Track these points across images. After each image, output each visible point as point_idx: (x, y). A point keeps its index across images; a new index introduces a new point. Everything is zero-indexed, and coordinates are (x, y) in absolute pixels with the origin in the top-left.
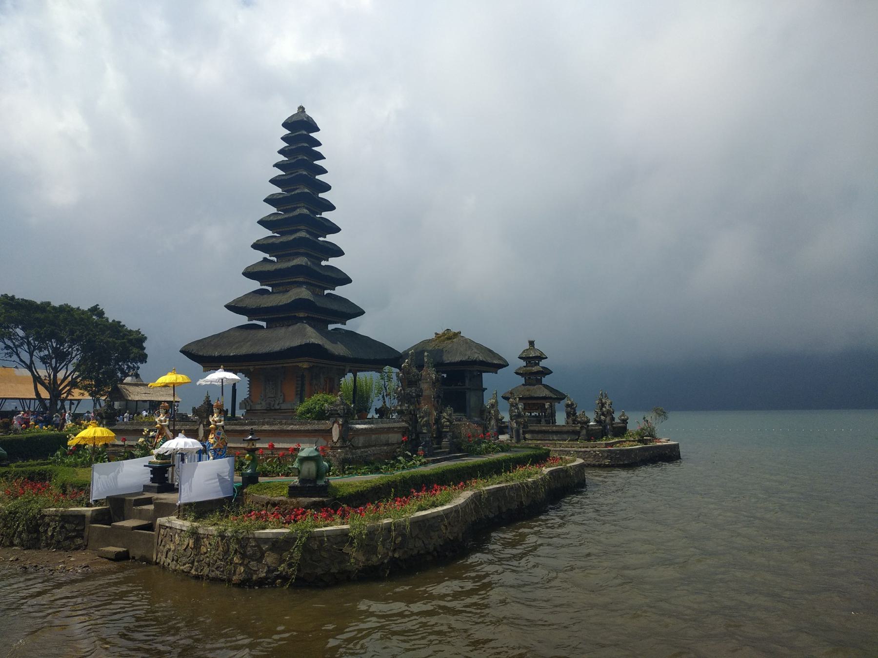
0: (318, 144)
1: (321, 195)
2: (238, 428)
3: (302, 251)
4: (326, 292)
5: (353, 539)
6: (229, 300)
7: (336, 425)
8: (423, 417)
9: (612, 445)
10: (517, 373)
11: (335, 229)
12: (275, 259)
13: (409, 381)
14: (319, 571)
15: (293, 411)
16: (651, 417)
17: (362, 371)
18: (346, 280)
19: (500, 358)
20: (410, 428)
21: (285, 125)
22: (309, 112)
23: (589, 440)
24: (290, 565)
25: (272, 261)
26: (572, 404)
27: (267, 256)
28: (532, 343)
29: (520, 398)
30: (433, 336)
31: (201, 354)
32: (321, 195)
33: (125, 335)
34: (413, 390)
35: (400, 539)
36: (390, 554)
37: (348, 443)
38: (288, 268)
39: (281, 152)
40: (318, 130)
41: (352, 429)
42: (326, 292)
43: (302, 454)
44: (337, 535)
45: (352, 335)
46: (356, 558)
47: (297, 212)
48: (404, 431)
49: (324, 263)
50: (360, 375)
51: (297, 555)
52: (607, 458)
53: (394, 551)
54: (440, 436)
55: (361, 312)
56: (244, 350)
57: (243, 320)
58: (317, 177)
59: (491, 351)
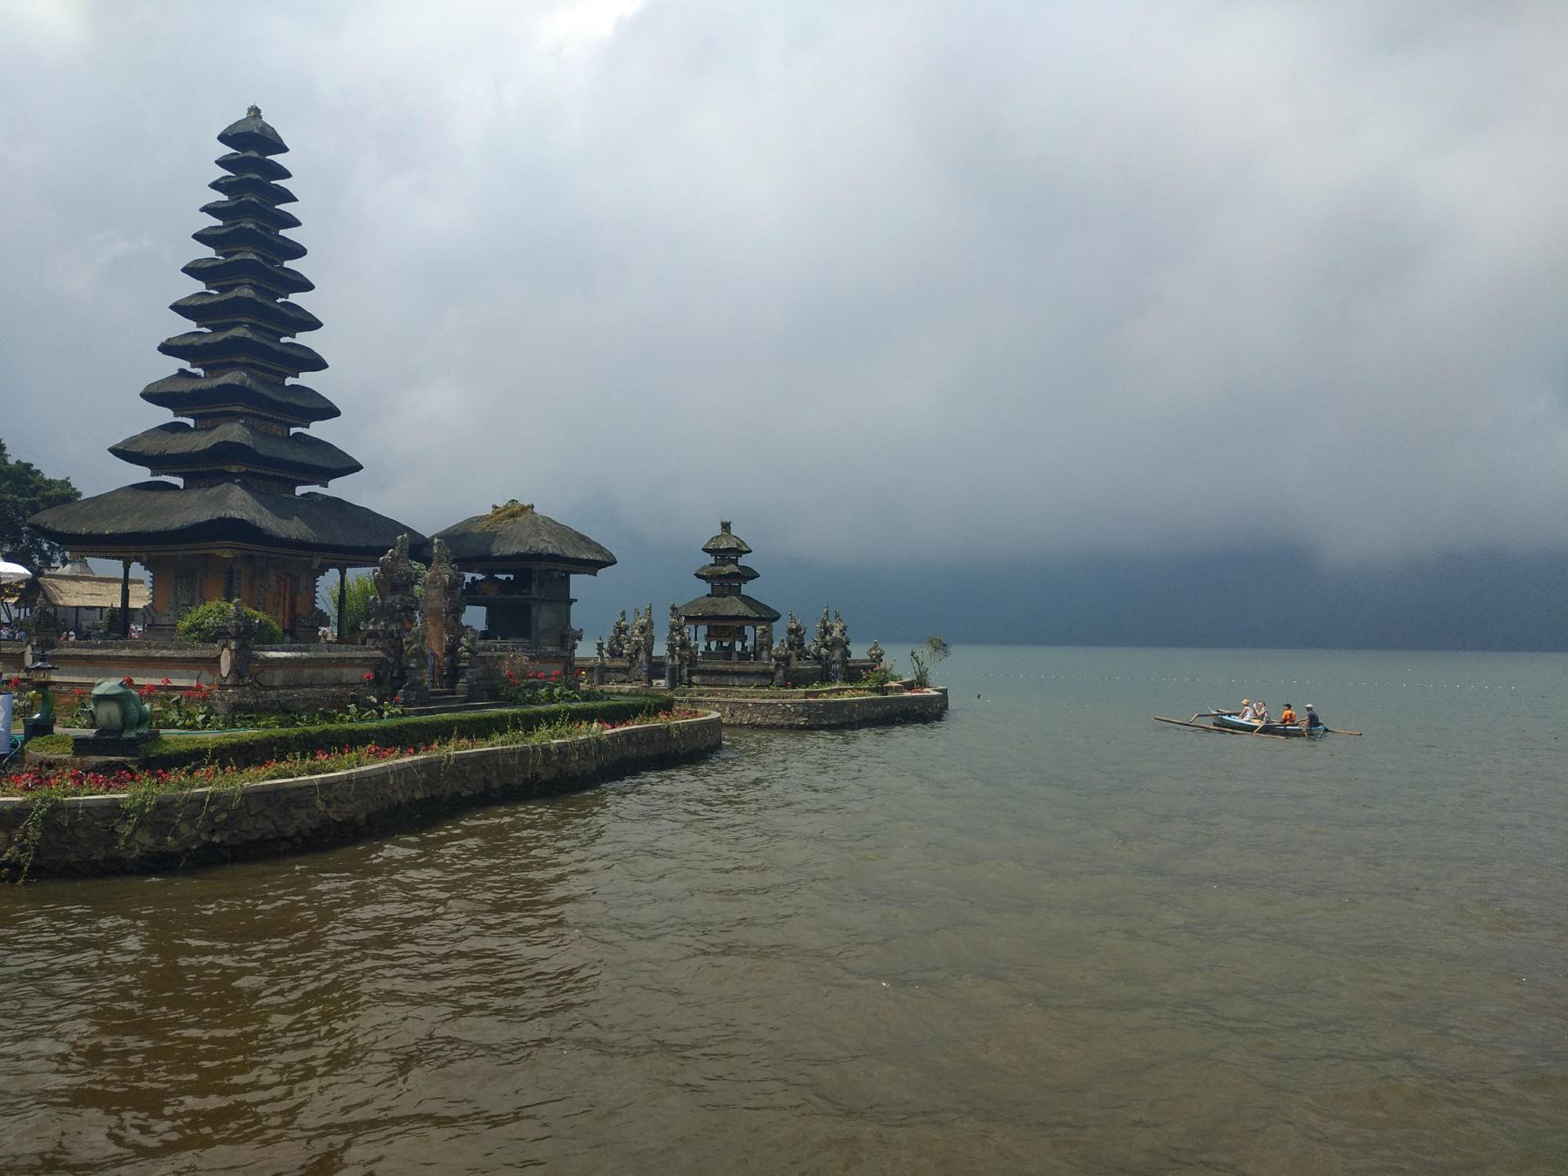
0: (286, 174)
1: (288, 264)
2: (85, 652)
3: (242, 359)
4: (293, 431)
5: (128, 811)
6: (116, 441)
7: (226, 651)
8: (411, 643)
9: (816, 694)
10: (697, 575)
11: (313, 324)
12: (200, 372)
13: (394, 583)
14: (72, 858)
15: (173, 628)
16: (924, 652)
17: (355, 566)
18: (330, 412)
19: (600, 549)
20: (391, 660)
21: (223, 138)
22: (267, 118)
23: (785, 686)
24: (23, 849)
25: (195, 376)
26: (799, 629)
27: (186, 365)
28: (726, 526)
29: (688, 619)
30: (489, 511)
31: (59, 529)
32: (288, 264)
33: (39, 488)
34: (395, 600)
35: (224, 816)
36: (204, 837)
37: (247, 680)
38: (211, 391)
39: (215, 186)
40: (284, 149)
41: (256, 659)
42: (293, 431)
43: (96, 691)
44: (104, 807)
45: (338, 504)
46: (134, 840)
47: (237, 292)
48: (377, 665)
49: (289, 381)
50: (353, 574)
51: (34, 834)
52: (802, 715)
53: (213, 832)
54: (454, 674)
55: (357, 467)
56: (127, 527)
57: (142, 474)
58: (282, 232)
59: (583, 538)
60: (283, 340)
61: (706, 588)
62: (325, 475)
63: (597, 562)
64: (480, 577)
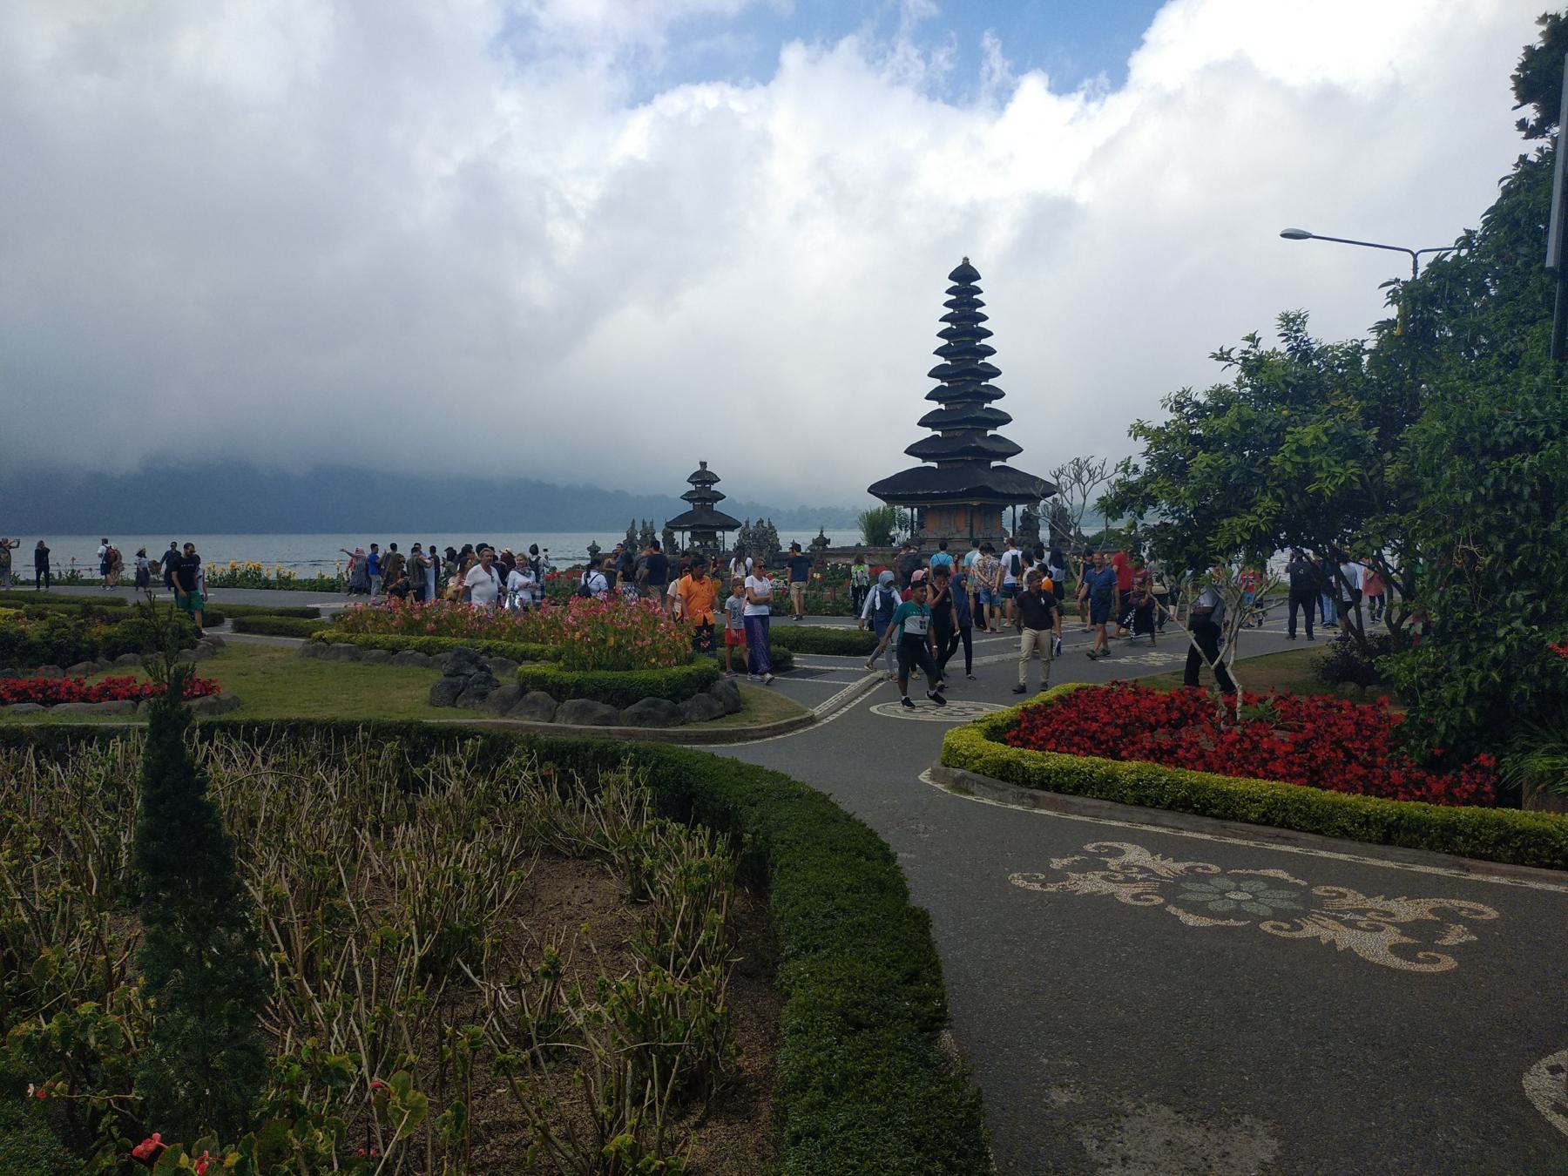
4: (989, 433)
11: (997, 373)
12: (943, 407)
40: (979, 278)
62: (1004, 456)
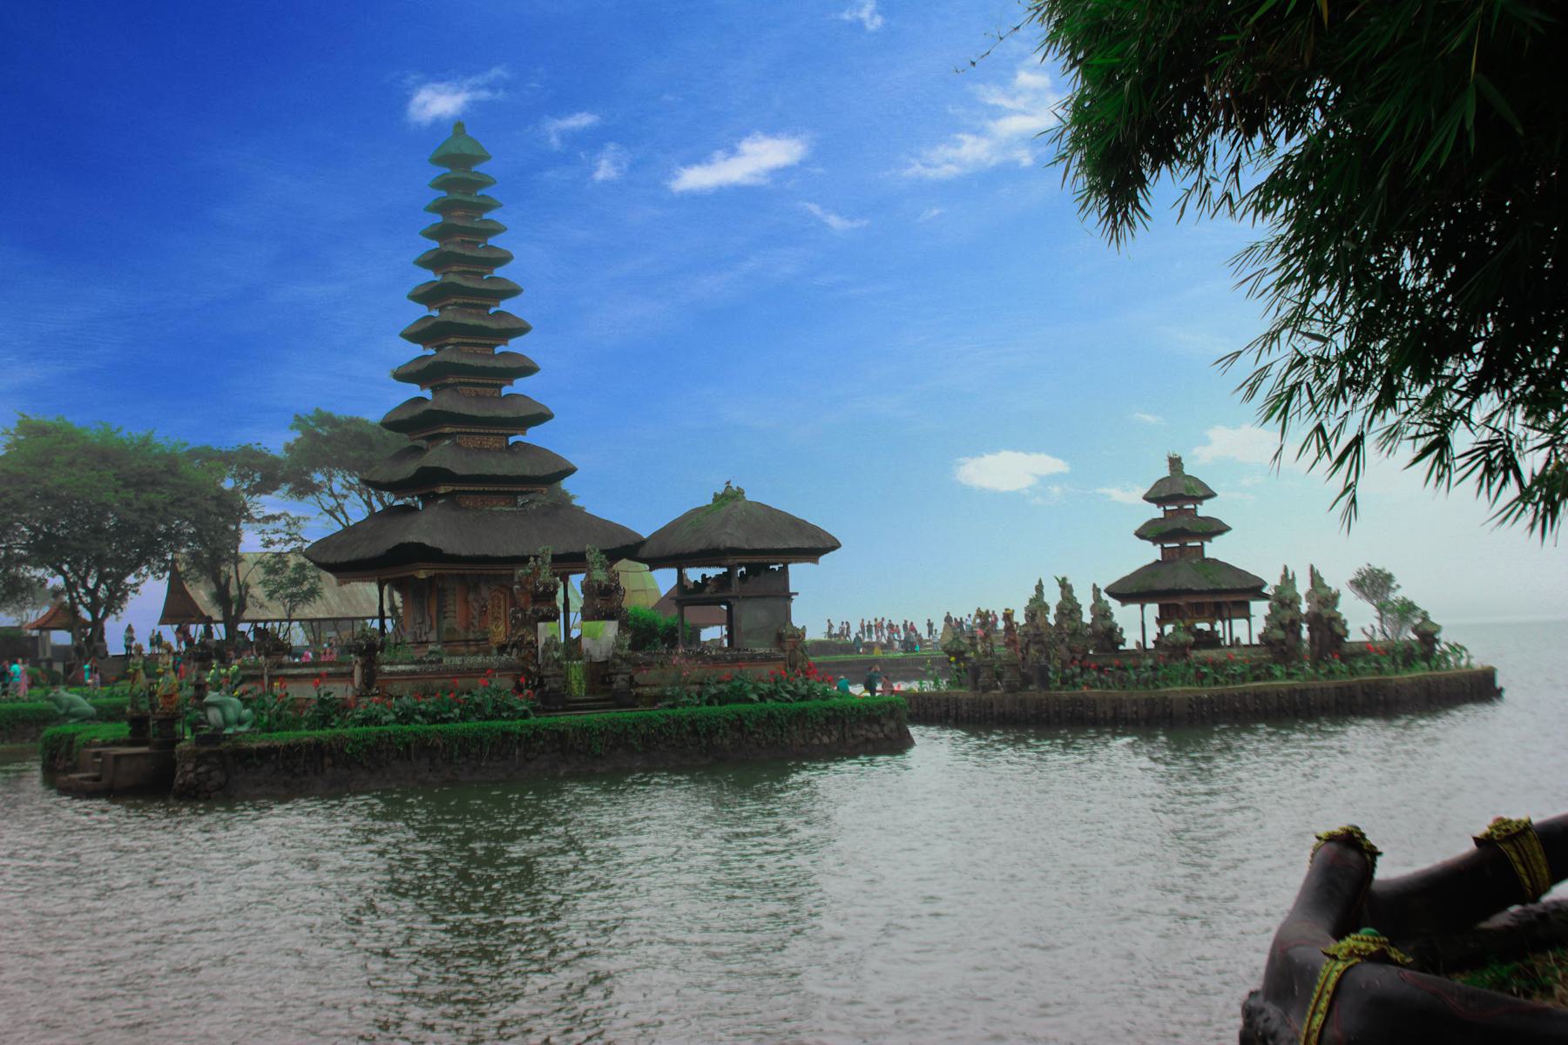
4: (512, 440)
19: (816, 532)
28: (1175, 463)
40: (484, 158)
42: (512, 440)
60: (498, 350)
61: (1151, 553)
63: (816, 546)
64: (712, 572)
